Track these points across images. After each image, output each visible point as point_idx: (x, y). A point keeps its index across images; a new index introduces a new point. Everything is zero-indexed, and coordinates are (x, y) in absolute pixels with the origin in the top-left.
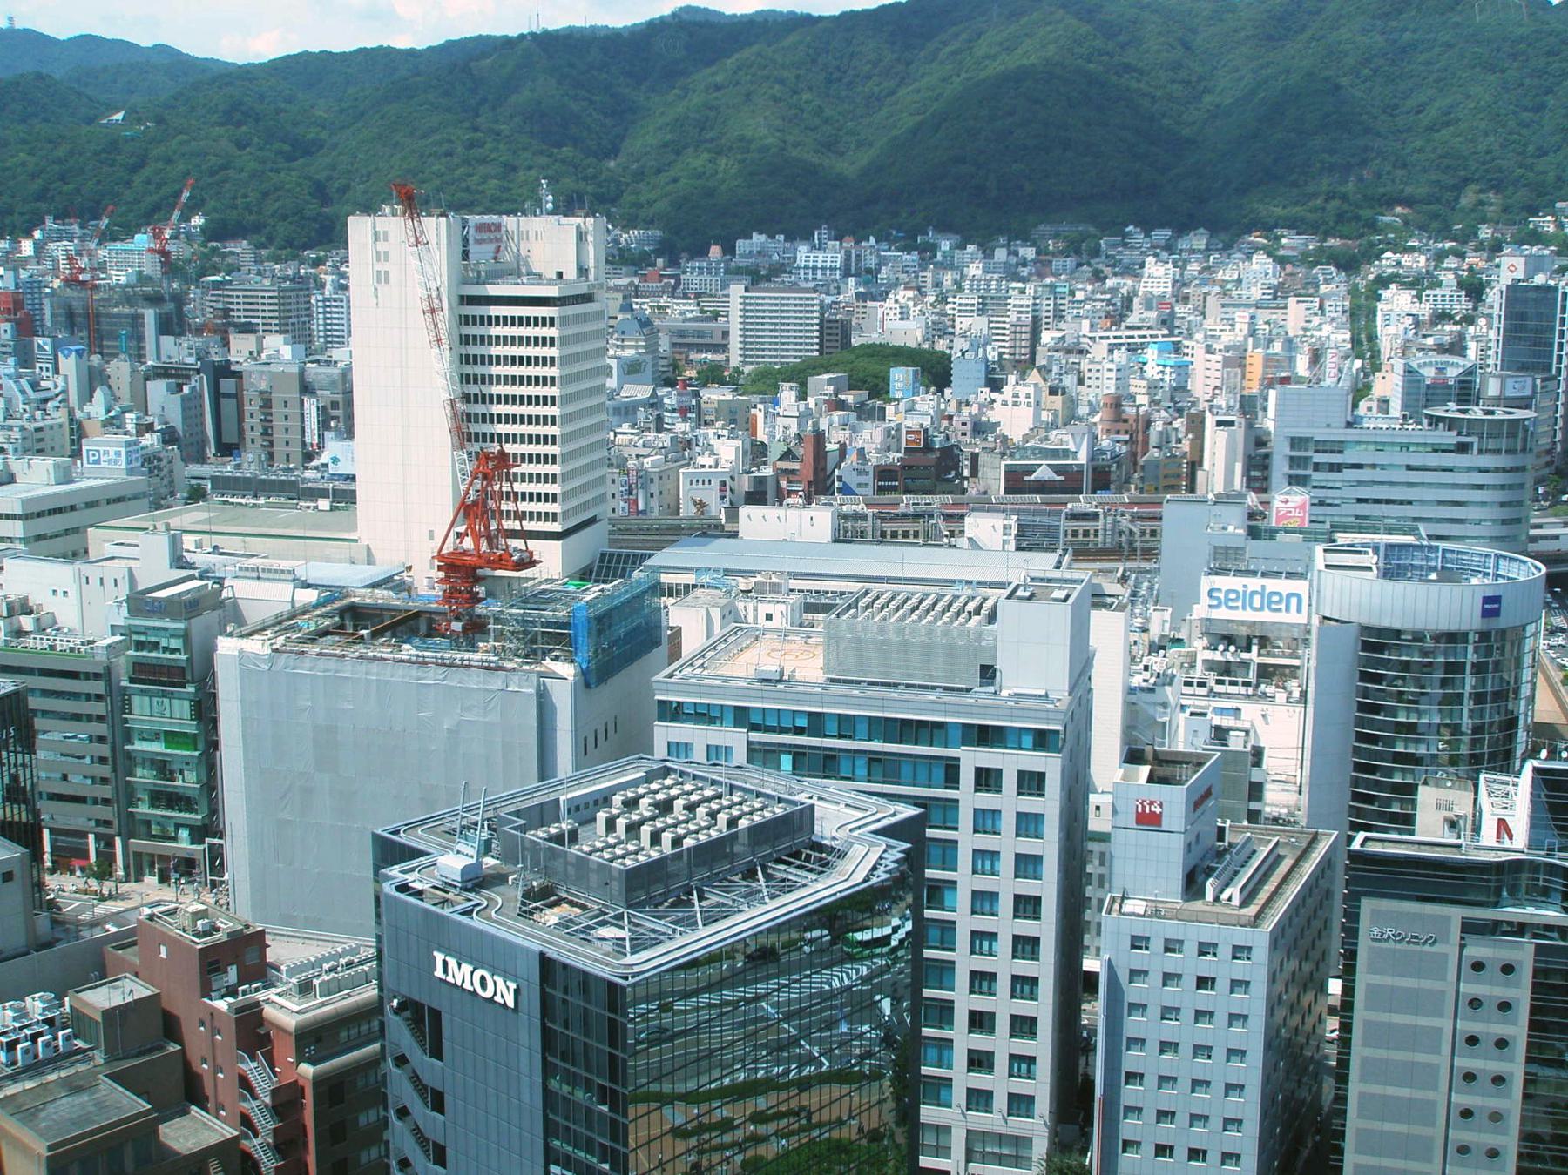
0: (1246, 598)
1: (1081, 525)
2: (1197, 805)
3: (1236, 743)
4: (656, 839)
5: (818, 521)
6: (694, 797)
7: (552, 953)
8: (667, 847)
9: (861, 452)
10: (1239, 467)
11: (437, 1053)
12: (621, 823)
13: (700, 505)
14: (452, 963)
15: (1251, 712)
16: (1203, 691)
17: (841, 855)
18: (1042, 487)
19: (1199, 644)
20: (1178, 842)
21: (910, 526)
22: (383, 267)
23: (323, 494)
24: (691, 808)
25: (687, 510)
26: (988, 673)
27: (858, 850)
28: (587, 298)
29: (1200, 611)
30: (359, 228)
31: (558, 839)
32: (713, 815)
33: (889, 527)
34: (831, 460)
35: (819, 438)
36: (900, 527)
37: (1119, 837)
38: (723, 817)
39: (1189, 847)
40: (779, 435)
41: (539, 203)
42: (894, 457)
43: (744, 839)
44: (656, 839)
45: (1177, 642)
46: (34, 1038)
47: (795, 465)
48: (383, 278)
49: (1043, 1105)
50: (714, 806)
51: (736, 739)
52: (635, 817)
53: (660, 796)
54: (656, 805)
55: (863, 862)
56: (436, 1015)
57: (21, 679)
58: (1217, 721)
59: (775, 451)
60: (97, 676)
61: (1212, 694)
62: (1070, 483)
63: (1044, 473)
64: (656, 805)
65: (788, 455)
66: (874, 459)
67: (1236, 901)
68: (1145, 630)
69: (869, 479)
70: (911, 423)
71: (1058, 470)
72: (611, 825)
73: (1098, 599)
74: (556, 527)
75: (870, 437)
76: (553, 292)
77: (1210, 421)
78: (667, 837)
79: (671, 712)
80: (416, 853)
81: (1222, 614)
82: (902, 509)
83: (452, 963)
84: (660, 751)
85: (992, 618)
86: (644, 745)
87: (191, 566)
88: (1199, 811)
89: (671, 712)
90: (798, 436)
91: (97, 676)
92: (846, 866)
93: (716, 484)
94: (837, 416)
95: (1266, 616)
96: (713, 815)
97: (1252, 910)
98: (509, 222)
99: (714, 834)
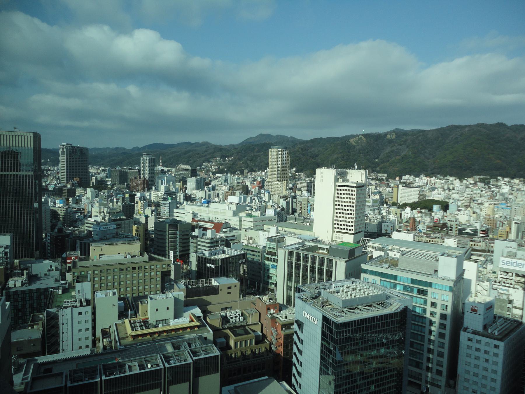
0: (512, 264)
1: (473, 243)
2: (487, 309)
3: (505, 297)
4: (351, 295)
5: (409, 237)
6: (362, 288)
7: (324, 314)
8: (353, 297)
9: (424, 223)
10: (520, 234)
11: (303, 333)
12: (345, 291)
13: (386, 230)
14: (306, 314)
15: (512, 291)
16: (499, 284)
17: (391, 305)
18: (468, 234)
19: (499, 273)
20: (481, 317)
21: (434, 240)
22: (322, 179)
23: (308, 222)
24: (360, 290)
25: (384, 231)
26: (436, 271)
27: (395, 304)
28: (363, 186)
29: (501, 266)
30: (318, 171)
31: (331, 292)
32: (364, 292)
33: (429, 239)
34: (417, 224)
35: (414, 219)
36: (431, 240)
37: (466, 313)
38: (366, 293)
39: (484, 319)
40: (406, 217)
41: (354, 167)
42: (432, 224)
43: (370, 297)
44: (351, 295)
45: (494, 273)
46: (236, 317)
47: (408, 224)
48: (322, 181)
49: (444, 373)
50: (365, 290)
51: (378, 279)
52: (348, 290)
53: (355, 287)
54: (353, 289)
55: (394, 307)
56: (303, 323)
57: (246, 251)
58: (500, 291)
59: (404, 221)
60: (259, 252)
61: (501, 285)
62: (475, 233)
63: (468, 231)
64: (353, 289)
65: (407, 222)
66: (426, 224)
67: (496, 334)
68: (486, 268)
69: (425, 229)
70: (436, 217)
71: (471, 230)
72: (343, 291)
73: (469, 259)
74: (353, 232)
75: (427, 219)
76: (355, 185)
77: (514, 222)
78: (353, 295)
79: (365, 271)
80: (303, 291)
81: (505, 267)
82: (432, 235)
83: (306, 314)
84: (362, 279)
85: (437, 260)
86: (359, 277)
87: (280, 233)
88: (488, 311)
89: (365, 271)
90: (410, 218)
91: (259, 252)
92: (391, 307)
93: (390, 227)
94: (419, 215)
95: (517, 268)
96: (364, 292)
97: (500, 337)
98: (348, 171)
99: (364, 296)
